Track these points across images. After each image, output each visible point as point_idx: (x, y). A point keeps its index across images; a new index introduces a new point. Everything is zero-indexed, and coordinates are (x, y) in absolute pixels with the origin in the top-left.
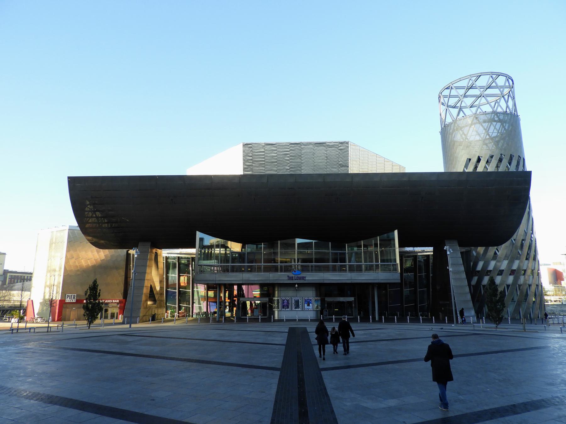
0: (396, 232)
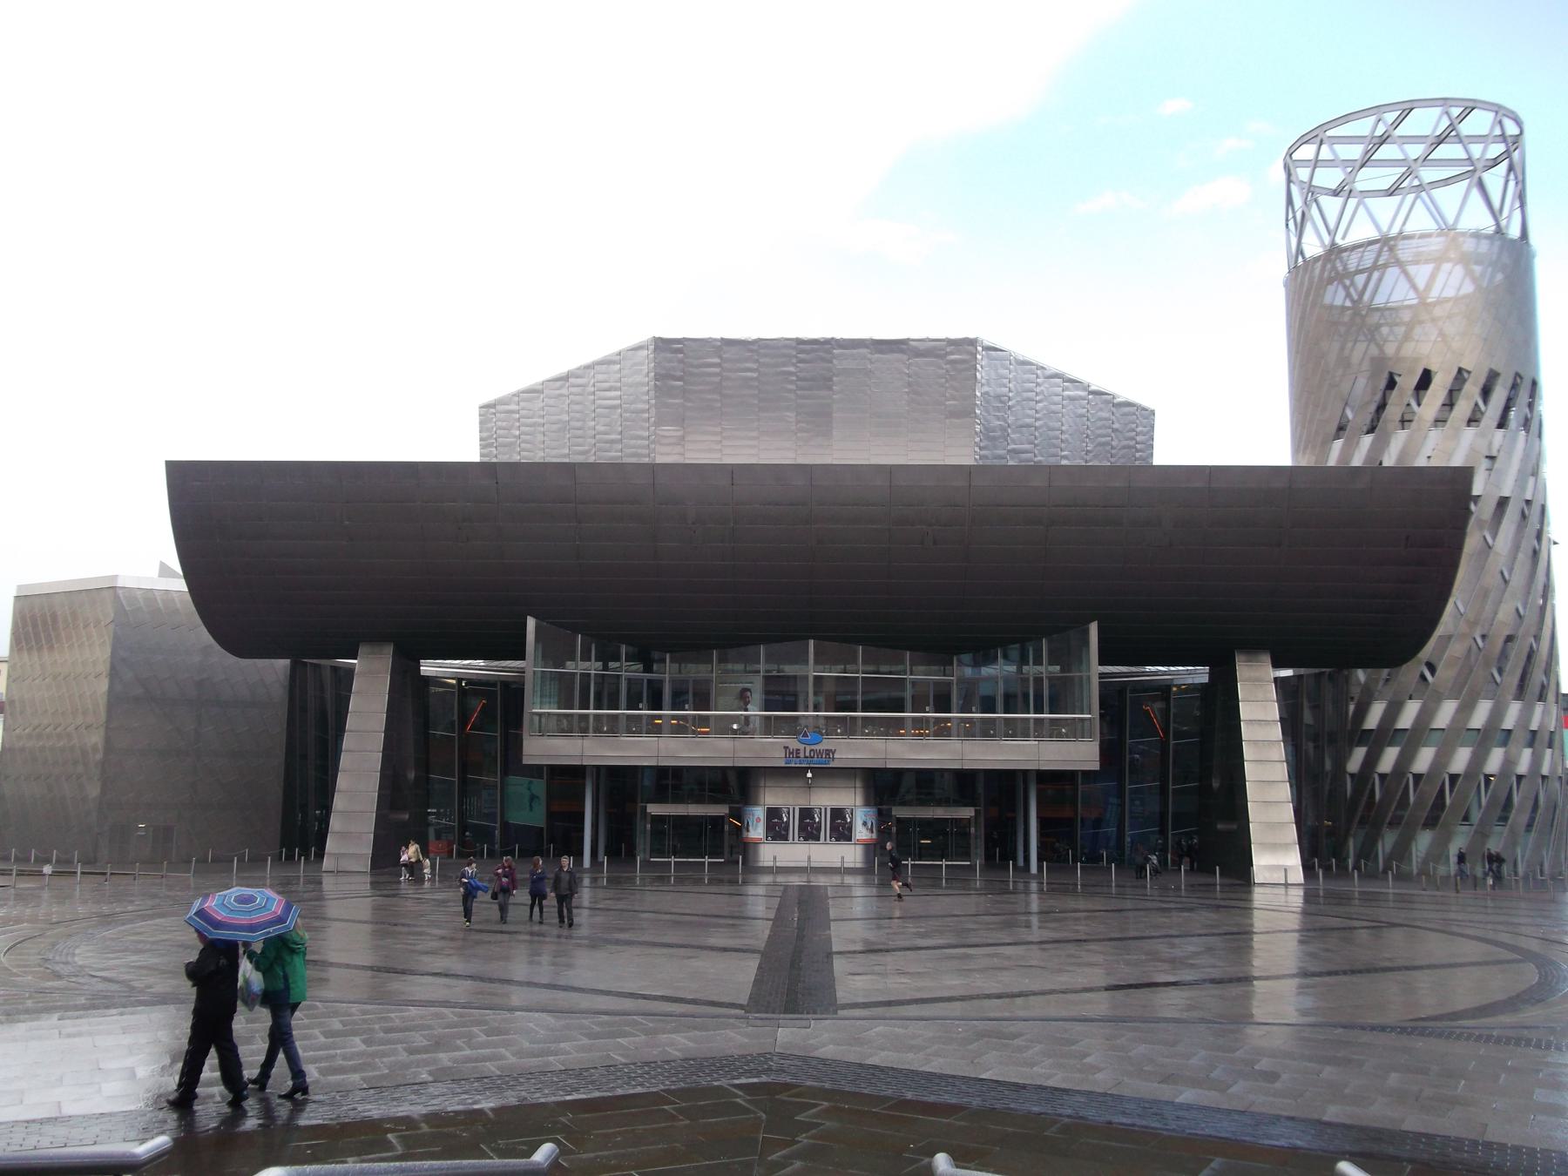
0: (1094, 628)
